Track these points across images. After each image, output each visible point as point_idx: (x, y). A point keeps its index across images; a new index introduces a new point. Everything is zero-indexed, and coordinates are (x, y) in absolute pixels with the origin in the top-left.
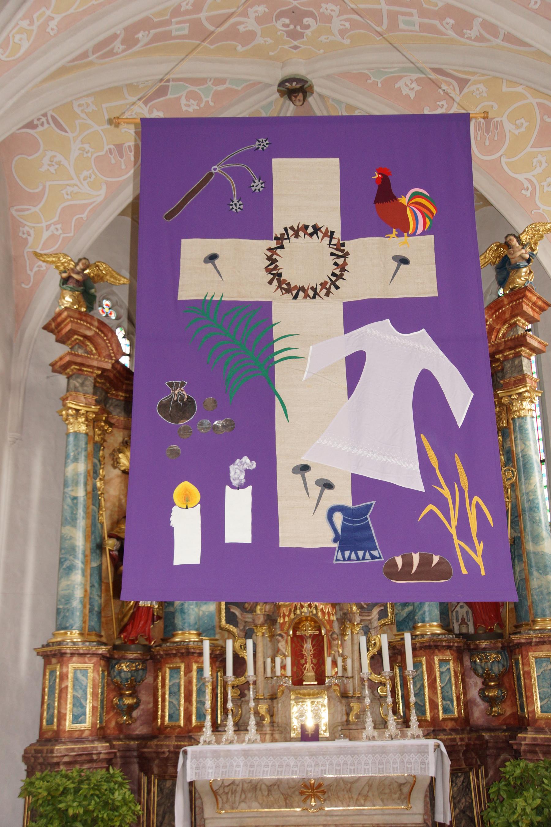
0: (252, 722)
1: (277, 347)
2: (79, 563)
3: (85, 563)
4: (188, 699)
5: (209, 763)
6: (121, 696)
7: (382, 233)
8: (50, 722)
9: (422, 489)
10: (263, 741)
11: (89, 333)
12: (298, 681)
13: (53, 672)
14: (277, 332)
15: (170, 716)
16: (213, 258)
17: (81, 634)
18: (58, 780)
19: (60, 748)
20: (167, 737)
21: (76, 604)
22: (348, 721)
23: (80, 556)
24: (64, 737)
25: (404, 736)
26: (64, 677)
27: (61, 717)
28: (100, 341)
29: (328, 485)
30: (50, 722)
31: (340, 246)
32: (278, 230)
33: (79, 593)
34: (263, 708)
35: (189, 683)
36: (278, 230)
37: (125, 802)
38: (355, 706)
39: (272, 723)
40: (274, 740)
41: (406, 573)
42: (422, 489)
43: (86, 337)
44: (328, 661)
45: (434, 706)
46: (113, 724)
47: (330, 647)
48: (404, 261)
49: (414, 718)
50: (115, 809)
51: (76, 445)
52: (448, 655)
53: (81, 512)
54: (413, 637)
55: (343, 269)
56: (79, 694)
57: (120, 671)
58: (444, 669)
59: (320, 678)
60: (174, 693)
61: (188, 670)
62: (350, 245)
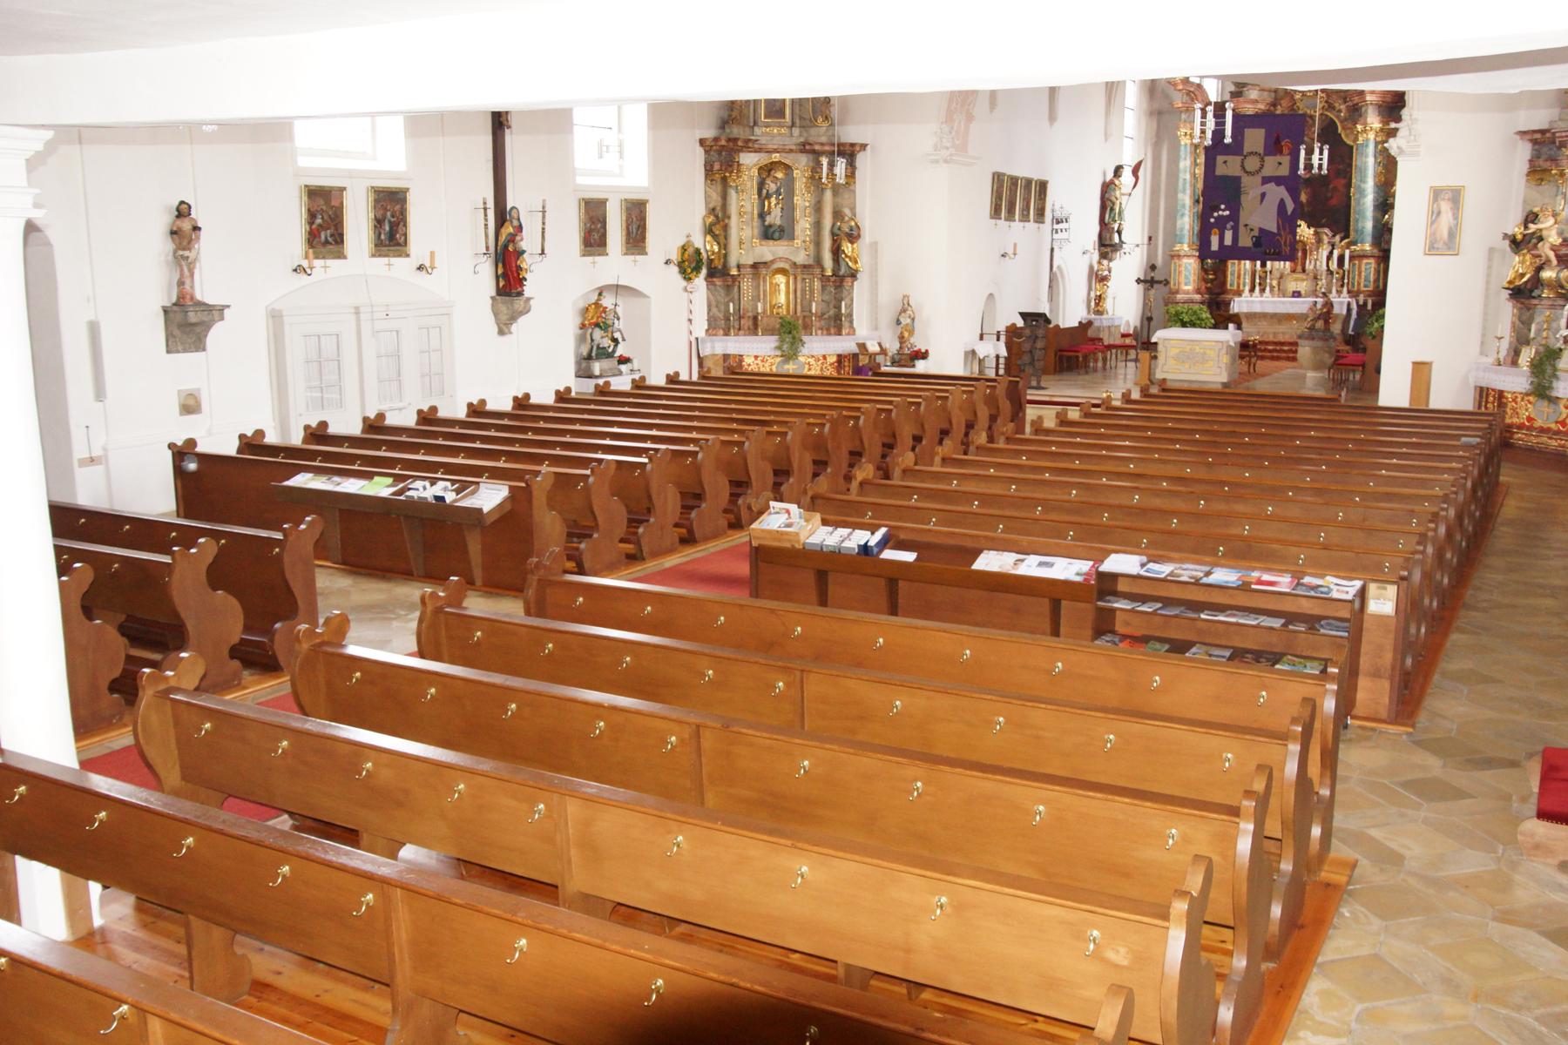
0: (1268, 289)
1: (1242, 189)
2: (1187, 212)
3: (1190, 211)
4: (1239, 277)
5: (1245, 305)
6: (1207, 274)
7: (1275, 155)
8: (1175, 285)
9: (1276, 231)
10: (1273, 297)
11: (1192, 89)
12: (1293, 271)
13: (1175, 263)
14: (1242, 185)
15: (1231, 285)
16: (1225, 162)
17: (1189, 246)
18: (1179, 308)
19: (1179, 297)
20: (1228, 294)
21: (1186, 232)
22: (1316, 290)
23: (1188, 208)
24: (1181, 292)
25: (1339, 297)
26: (1180, 266)
27: (1179, 283)
28: (1197, 93)
29: (1252, 230)
30: (1175, 285)
31: (1262, 159)
32: (1245, 154)
33: (1187, 227)
34: (1275, 283)
35: (1239, 270)
36: (1245, 154)
37: (1207, 318)
38: (1320, 283)
39: (1279, 289)
40: (1279, 297)
41: (1269, 254)
42: (1276, 231)
43: (1190, 91)
44: (1308, 262)
45: (1359, 284)
46: (1203, 287)
47: (1311, 255)
48: (1280, 164)
49: (1345, 289)
50: (1203, 320)
51: (1186, 151)
52: (1372, 261)
53: (1188, 185)
54: (1351, 252)
55: (1263, 165)
56: (1187, 274)
57: (1207, 263)
58: (1368, 267)
59: (1304, 271)
60: (1232, 274)
61: (1239, 264)
62: (1266, 158)
